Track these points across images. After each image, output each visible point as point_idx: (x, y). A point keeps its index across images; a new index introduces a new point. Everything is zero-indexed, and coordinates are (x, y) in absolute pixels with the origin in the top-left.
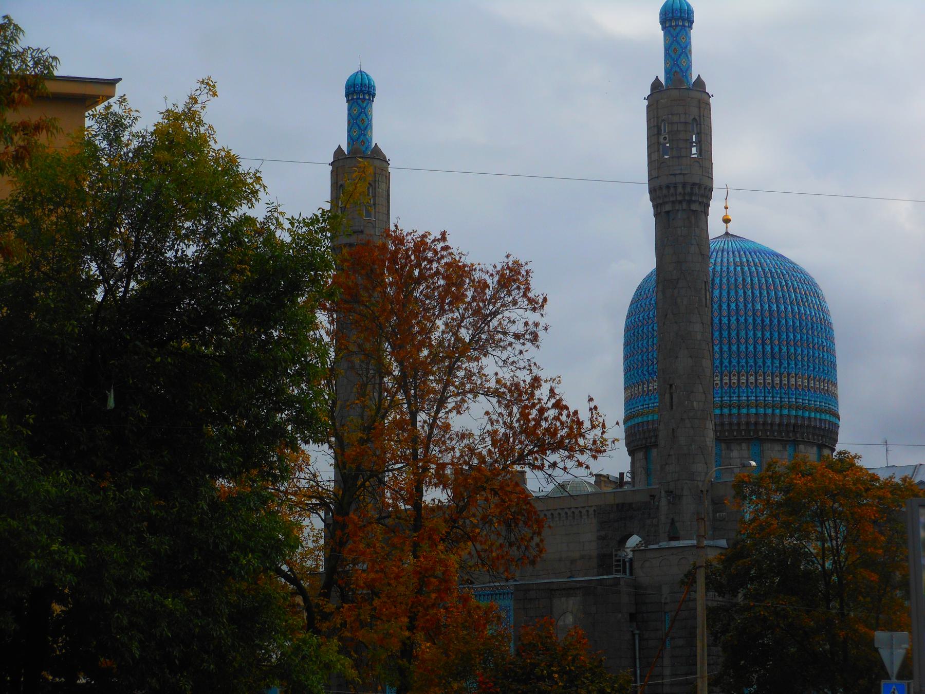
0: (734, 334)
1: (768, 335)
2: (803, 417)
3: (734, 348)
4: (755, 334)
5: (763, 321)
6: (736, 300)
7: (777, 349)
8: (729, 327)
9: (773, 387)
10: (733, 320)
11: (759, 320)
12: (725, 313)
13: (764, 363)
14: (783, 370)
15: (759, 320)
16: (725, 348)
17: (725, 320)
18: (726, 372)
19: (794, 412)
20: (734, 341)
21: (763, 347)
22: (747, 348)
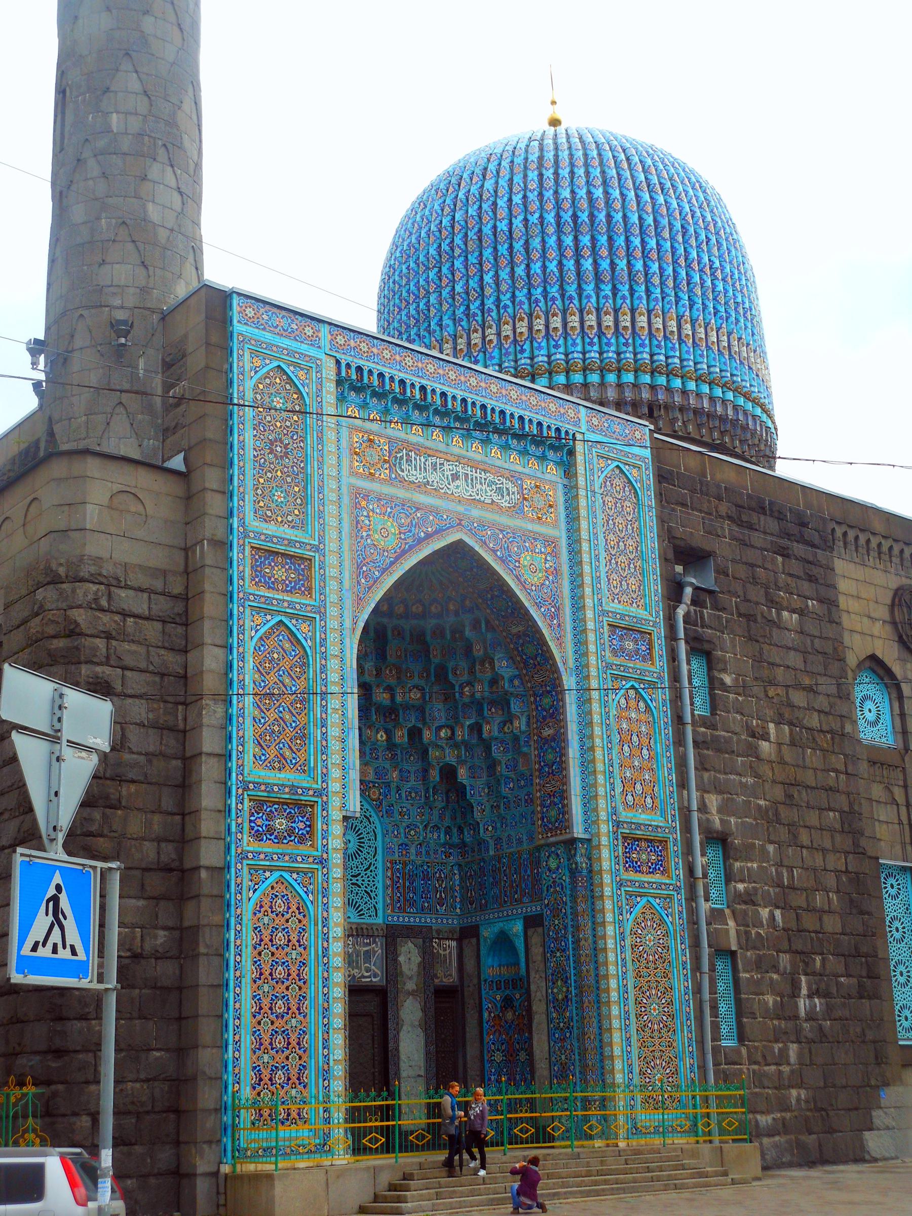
0: (518, 246)
1: (585, 240)
2: (668, 389)
3: (520, 271)
4: (560, 242)
5: (575, 217)
6: (525, 188)
7: (605, 265)
8: (511, 237)
9: (601, 334)
10: (518, 222)
11: (567, 217)
12: (503, 212)
13: (580, 289)
14: (619, 302)
15: (567, 217)
16: (504, 274)
17: (503, 226)
18: (506, 317)
19: (647, 379)
20: (520, 258)
21: (578, 264)
22: (544, 267)
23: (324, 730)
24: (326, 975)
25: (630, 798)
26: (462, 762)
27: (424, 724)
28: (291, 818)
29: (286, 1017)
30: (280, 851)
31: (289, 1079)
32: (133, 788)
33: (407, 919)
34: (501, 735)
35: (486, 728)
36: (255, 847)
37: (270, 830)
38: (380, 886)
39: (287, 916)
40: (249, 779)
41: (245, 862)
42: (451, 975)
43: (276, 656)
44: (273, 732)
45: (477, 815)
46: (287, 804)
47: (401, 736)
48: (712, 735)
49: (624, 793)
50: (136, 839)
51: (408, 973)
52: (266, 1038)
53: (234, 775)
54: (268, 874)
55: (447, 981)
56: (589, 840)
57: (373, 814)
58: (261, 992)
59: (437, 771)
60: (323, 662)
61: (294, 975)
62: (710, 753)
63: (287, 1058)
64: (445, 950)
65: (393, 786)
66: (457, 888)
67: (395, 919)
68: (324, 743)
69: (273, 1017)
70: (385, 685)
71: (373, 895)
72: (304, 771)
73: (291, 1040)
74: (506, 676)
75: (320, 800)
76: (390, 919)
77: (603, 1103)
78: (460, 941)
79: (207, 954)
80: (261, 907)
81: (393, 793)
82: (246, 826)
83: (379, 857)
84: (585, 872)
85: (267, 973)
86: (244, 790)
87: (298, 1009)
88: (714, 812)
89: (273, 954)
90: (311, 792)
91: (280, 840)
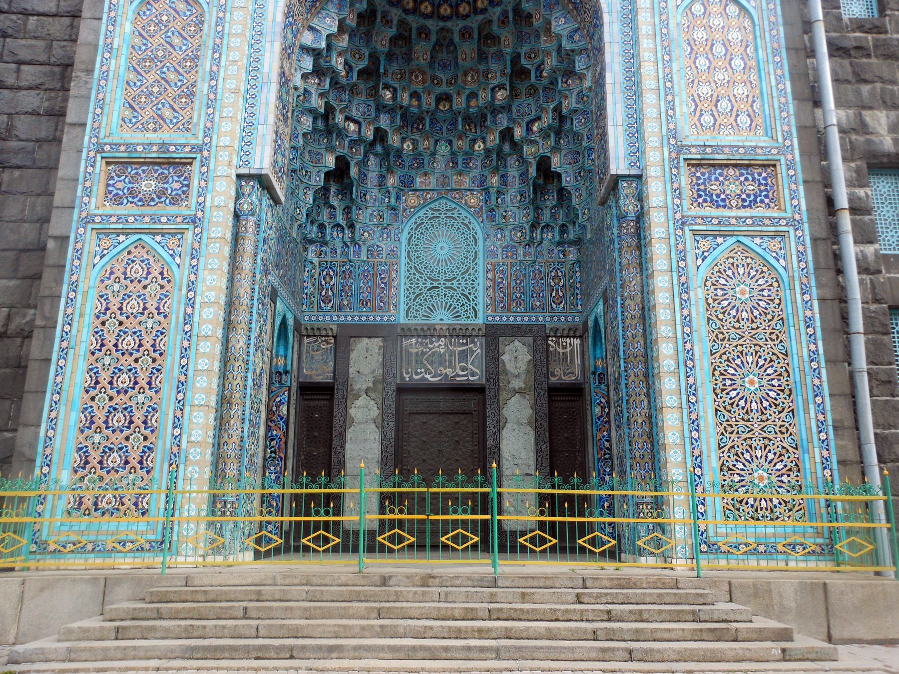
23: (213, 83)
24: (186, 344)
25: (707, 119)
26: (556, 149)
27: (514, 121)
28: (164, 179)
29: (131, 393)
30: (139, 213)
31: (127, 462)
32: (17, 173)
33: (512, 319)
34: (580, 106)
35: (565, 103)
36: (109, 209)
37: (133, 193)
38: (481, 288)
39: (144, 282)
40: (105, 141)
41: (90, 226)
42: (573, 373)
43: (165, 18)
44: (151, 93)
45: (575, 201)
46: (158, 164)
47: (493, 139)
48: (877, 40)
49: (697, 111)
50: (15, 221)
51: (515, 372)
52: (100, 416)
53: (86, 139)
54: (122, 238)
55: (566, 379)
56: (639, 177)
57: (472, 220)
58: (99, 365)
59: (534, 167)
60: (221, 15)
61: (148, 346)
62: (874, 60)
63: (127, 439)
64: (565, 347)
65: (493, 191)
66: (578, 285)
67: (497, 318)
68: (212, 96)
69: (113, 393)
70: (467, 92)
71: (471, 297)
72: (188, 130)
73: (135, 419)
74: (565, 33)
75: (199, 156)
76: (490, 319)
77: (658, 505)
78: (581, 337)
79: (44, 327)
80: (112, 273)
81: (493, 197)
82: (99, 190)
83: (480, 261)
84: (632, 216)
85: (111, 344)
86: (98, 152)
87: (149, 383)
88: (886, 133)
89: (121, 323)
90: (187, 149)
91: (145, 202)
